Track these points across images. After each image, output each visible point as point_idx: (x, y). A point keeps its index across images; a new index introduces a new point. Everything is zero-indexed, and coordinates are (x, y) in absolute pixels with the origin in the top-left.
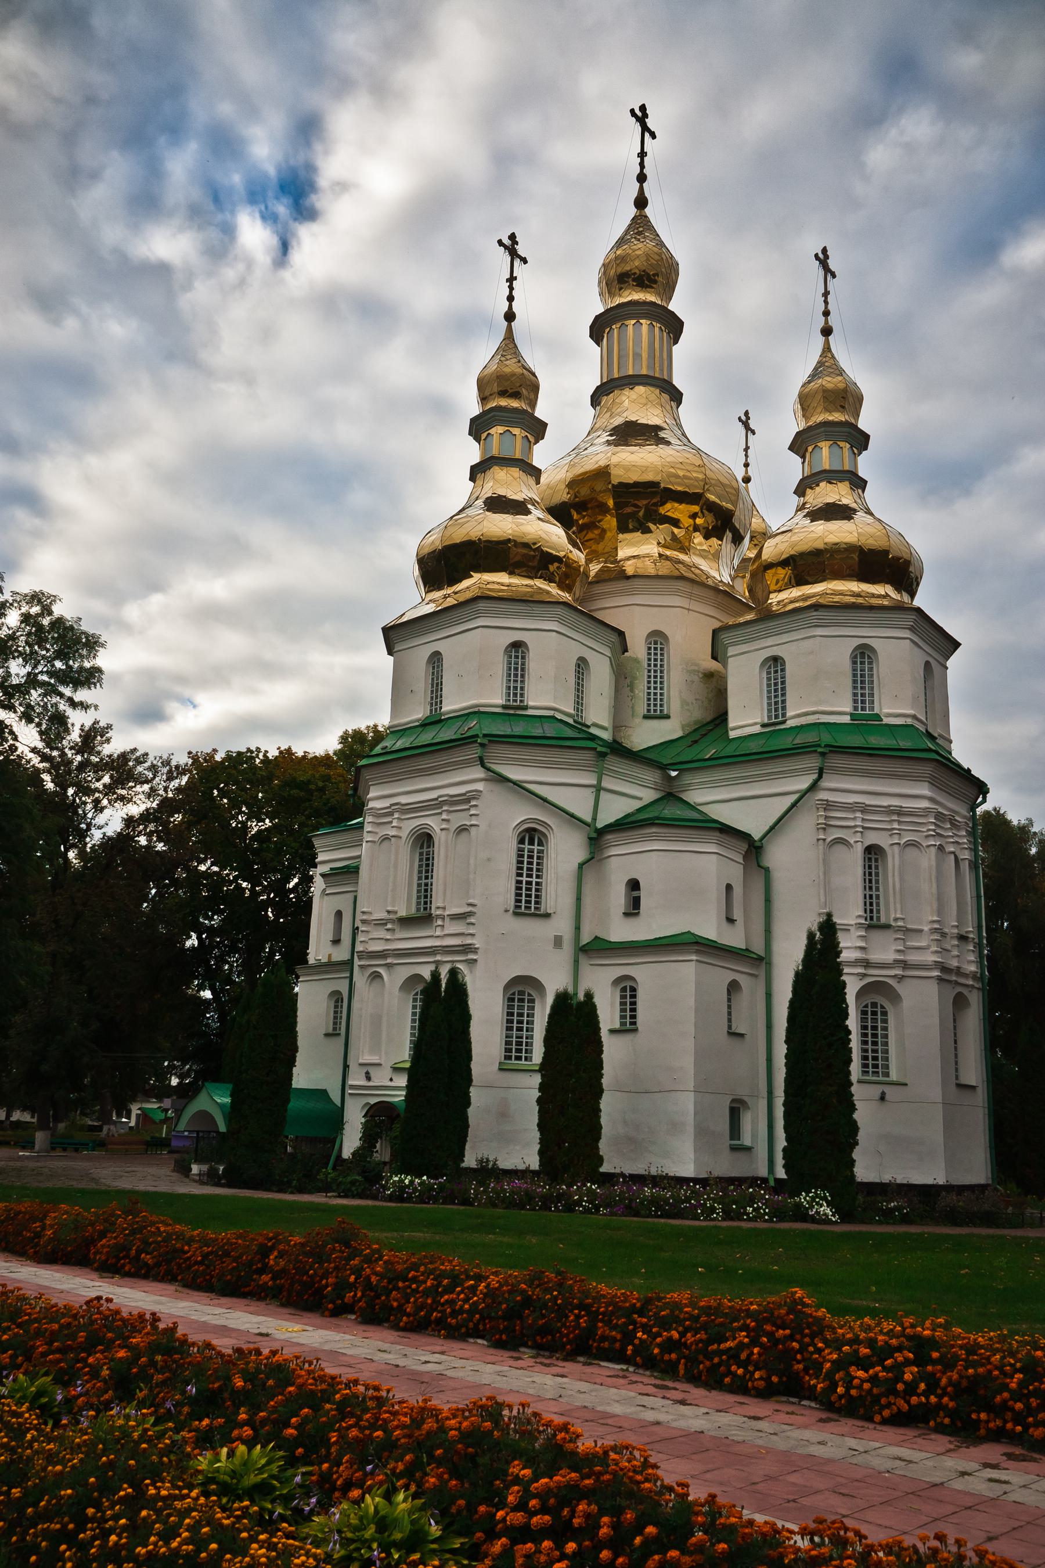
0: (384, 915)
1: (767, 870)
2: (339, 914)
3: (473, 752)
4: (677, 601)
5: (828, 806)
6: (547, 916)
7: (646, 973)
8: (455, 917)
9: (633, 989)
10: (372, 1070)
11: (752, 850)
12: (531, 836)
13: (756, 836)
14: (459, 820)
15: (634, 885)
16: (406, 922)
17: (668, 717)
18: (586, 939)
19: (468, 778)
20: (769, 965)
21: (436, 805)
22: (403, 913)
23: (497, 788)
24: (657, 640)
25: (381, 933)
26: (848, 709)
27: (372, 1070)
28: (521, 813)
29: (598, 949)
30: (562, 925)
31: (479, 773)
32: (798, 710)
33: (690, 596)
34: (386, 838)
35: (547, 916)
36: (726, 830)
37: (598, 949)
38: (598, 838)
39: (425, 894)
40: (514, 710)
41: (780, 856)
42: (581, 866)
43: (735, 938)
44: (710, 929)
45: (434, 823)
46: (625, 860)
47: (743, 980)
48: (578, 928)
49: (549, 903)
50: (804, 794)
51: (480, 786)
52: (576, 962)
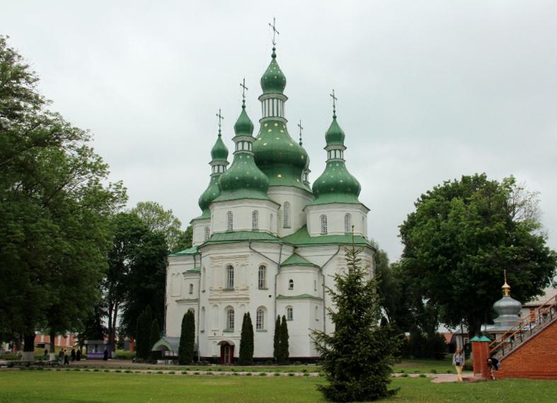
0: (218, 288)
1: (324, 276)
2: (192, 285)
3: (247, 244)
4: (292, 193)
5: (340, 259)
6: (267, 289)
7: (296, 305)
8: (242, 290)
9: (291, 309)
10: (216, 332)
11: (320, 270)
12: (262, 267)
13: (321, 266)
14: (241, 262)
15: (291, 281)
16: (226, 290)
17: (290, 228)
18: (277, 295)
19: (243, 250)
20: (324, 301)
21: (235, 257)
22: (224, 287)
23: (254, 254)
24: (287, 204)
25: (217, 293)
26: (344, 231)
27: (216, 332)
28: (261, 261)
29: (280, 298)
30: (271, 292)
31: (248, 249)
32: (330, 231)
33: (296, 191)
34: (216, 266)
35: (267, 289)
36: (316, 266)
37: (280, 298)
38: (281, 266)
39: (231, 282)
40: (255, 231)
41: (325, 272)
42: (276, 276)
43: (316, 295)
44: (312, 293)
45: (233, 263)
46: (288, 274)
47: (318, 305)
48: (275, 293)
49: (267, 286)
50: (334, 255)
51: (248, 253)
52: (276, 302)
